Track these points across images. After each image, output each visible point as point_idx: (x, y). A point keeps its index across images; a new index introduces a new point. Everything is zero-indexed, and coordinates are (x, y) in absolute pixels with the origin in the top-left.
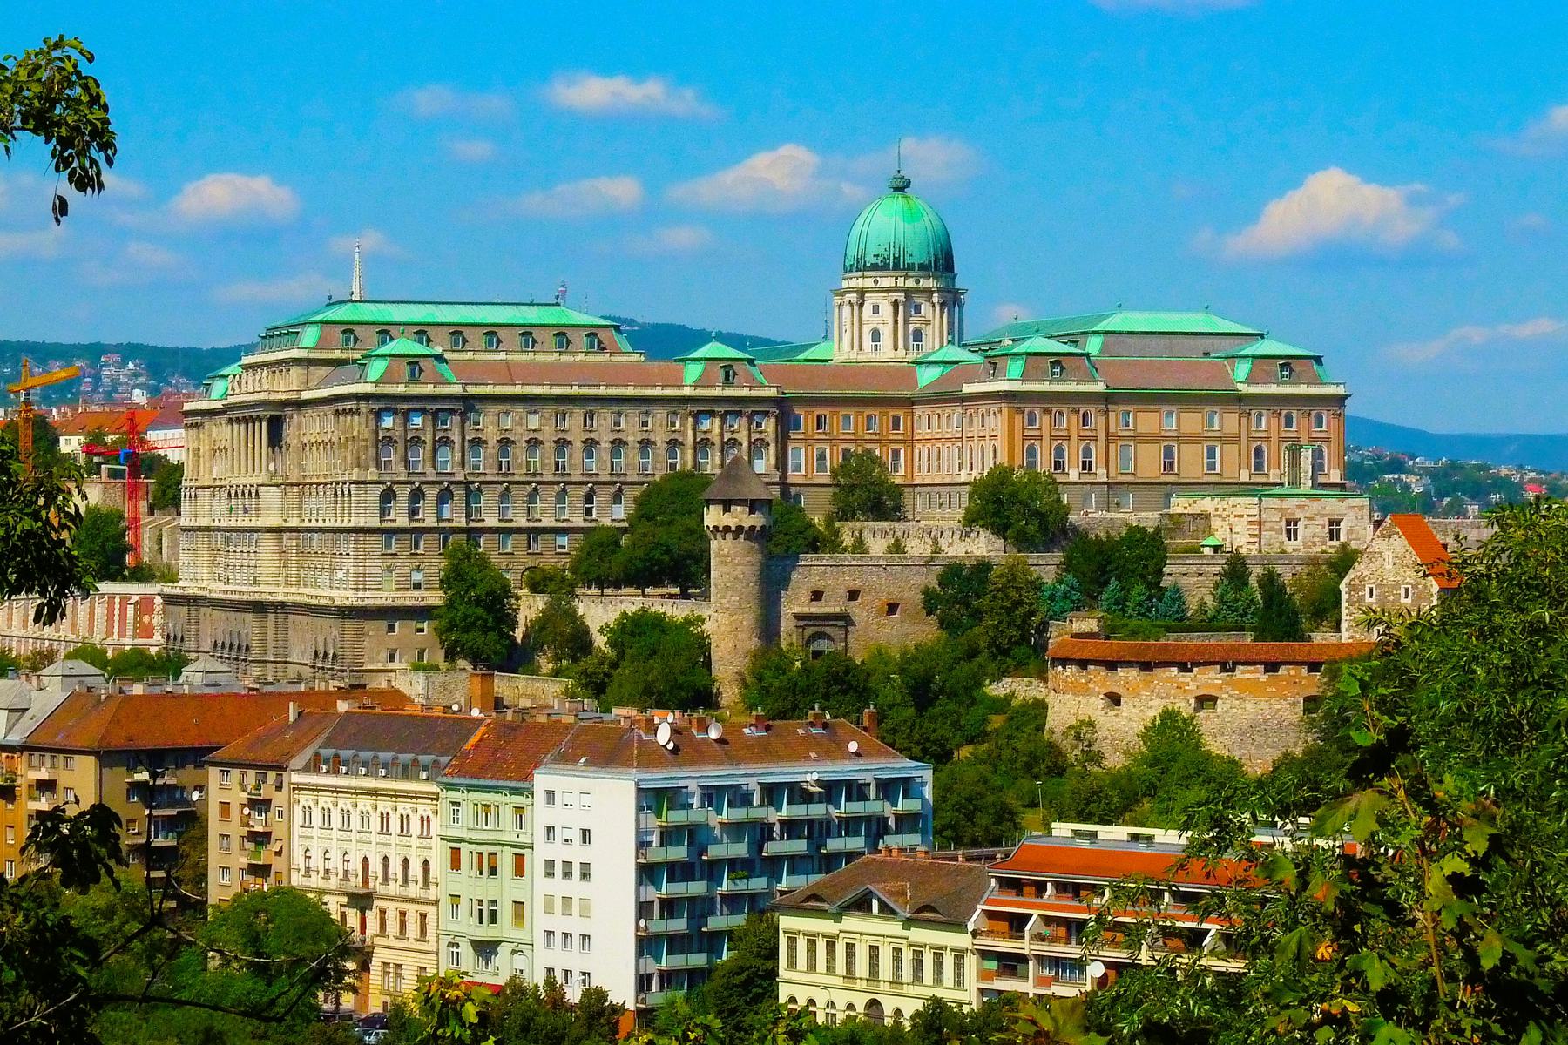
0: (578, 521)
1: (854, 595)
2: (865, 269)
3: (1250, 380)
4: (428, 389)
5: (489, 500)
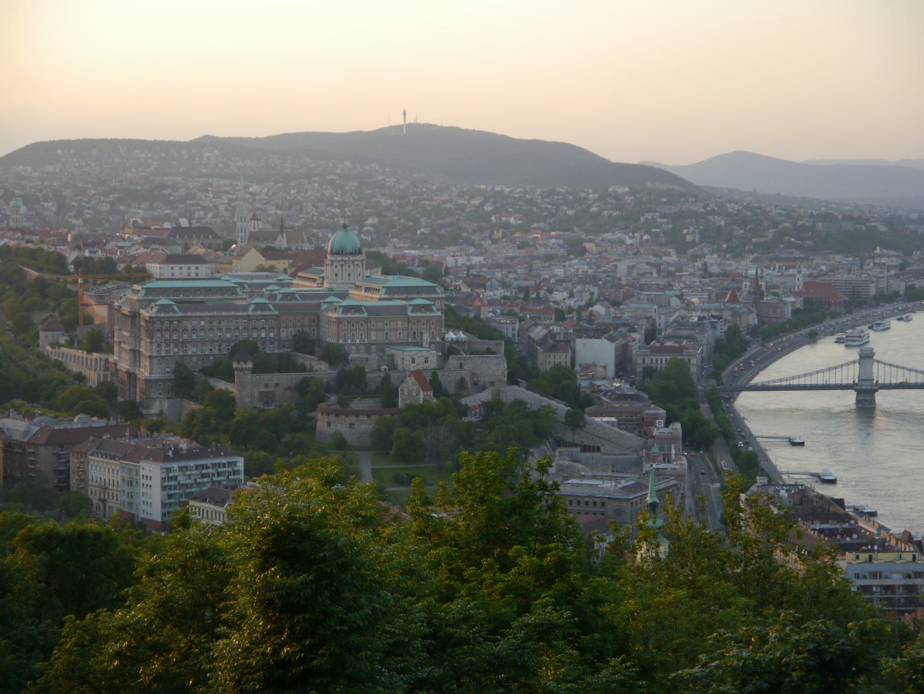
0: (216, 352)
1: (277, 385)
3: (412, 311)
4: (171, 314)
5: (189, 346)
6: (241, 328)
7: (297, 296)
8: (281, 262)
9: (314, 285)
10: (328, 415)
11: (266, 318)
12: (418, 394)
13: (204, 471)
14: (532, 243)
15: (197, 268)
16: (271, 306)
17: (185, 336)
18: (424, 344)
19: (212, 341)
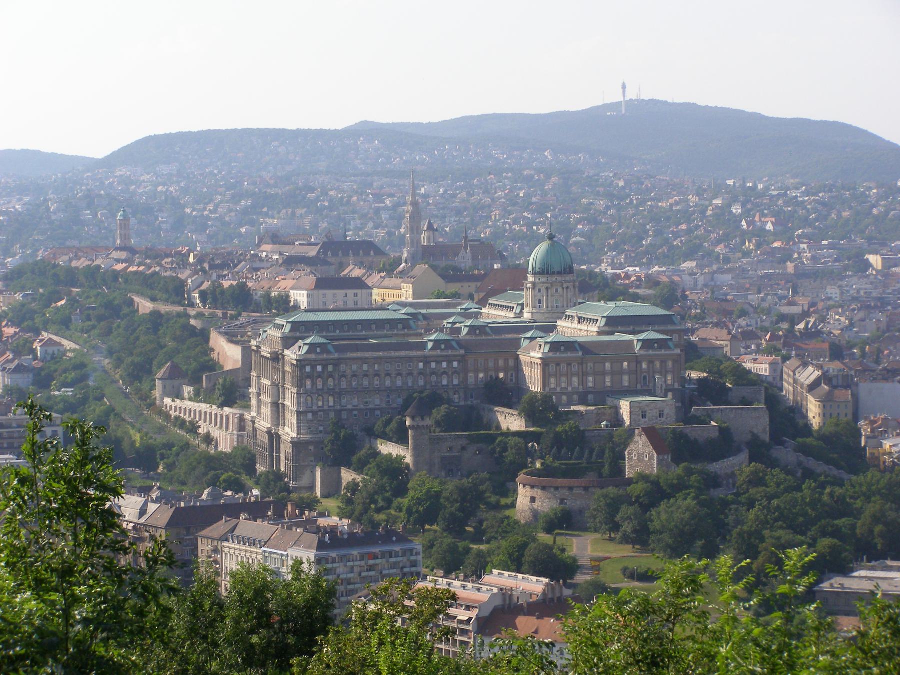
2: (536, 274)
4: (325, 356)
6: (415, 373)
7: (488, 329)
8: (466, 285)
9: (512, 315)
10: (533, 487)
11: (449, 360)
12: (651, 458)
13: (371, 562)
14: (796, 256)
15: (356, 295)
16: (454, 344)
17: (344, 385)
18: (658, 392)
19: (378, 391)
